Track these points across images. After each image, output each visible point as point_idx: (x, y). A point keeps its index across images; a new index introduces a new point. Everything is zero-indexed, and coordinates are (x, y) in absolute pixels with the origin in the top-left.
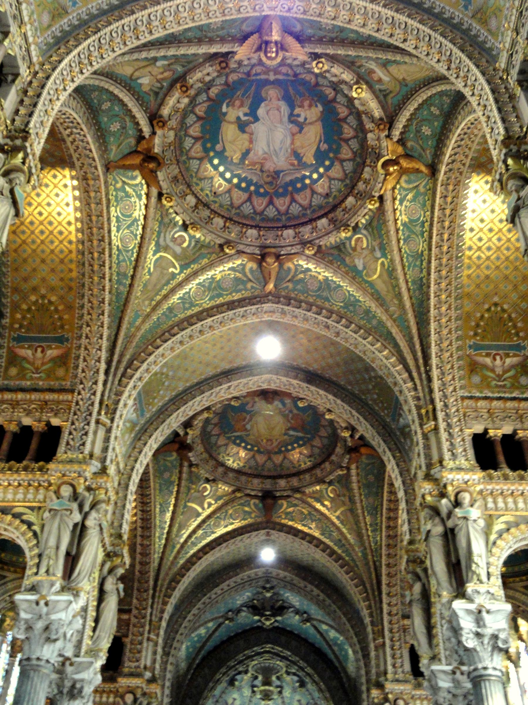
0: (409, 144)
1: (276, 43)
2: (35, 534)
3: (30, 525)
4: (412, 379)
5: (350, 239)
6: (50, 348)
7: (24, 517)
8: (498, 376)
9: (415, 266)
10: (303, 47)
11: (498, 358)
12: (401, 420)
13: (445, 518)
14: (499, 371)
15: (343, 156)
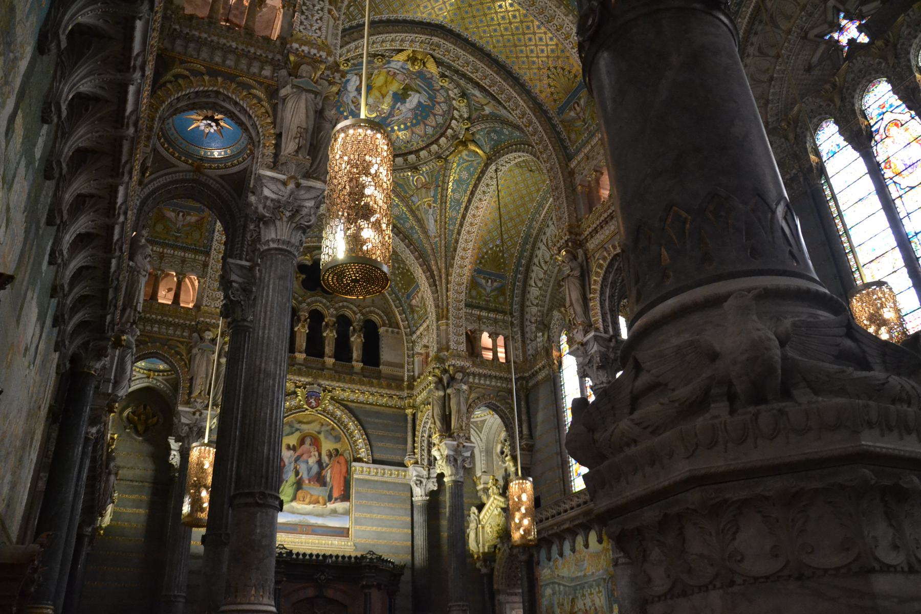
0: (478, 136)
1: (421, 60)
2: (186, 364)
3: (181, 355)
4: (436, 285)
5: (413, 177)
6: (189, 214)
7: (177, 349)
8: (488, 294)
9: (455, 209)
10: (438, 67)
11: (490, 281)
12: (414, 301)
13: (446, 384)
14: (489, 290)
15: (428, 122)
